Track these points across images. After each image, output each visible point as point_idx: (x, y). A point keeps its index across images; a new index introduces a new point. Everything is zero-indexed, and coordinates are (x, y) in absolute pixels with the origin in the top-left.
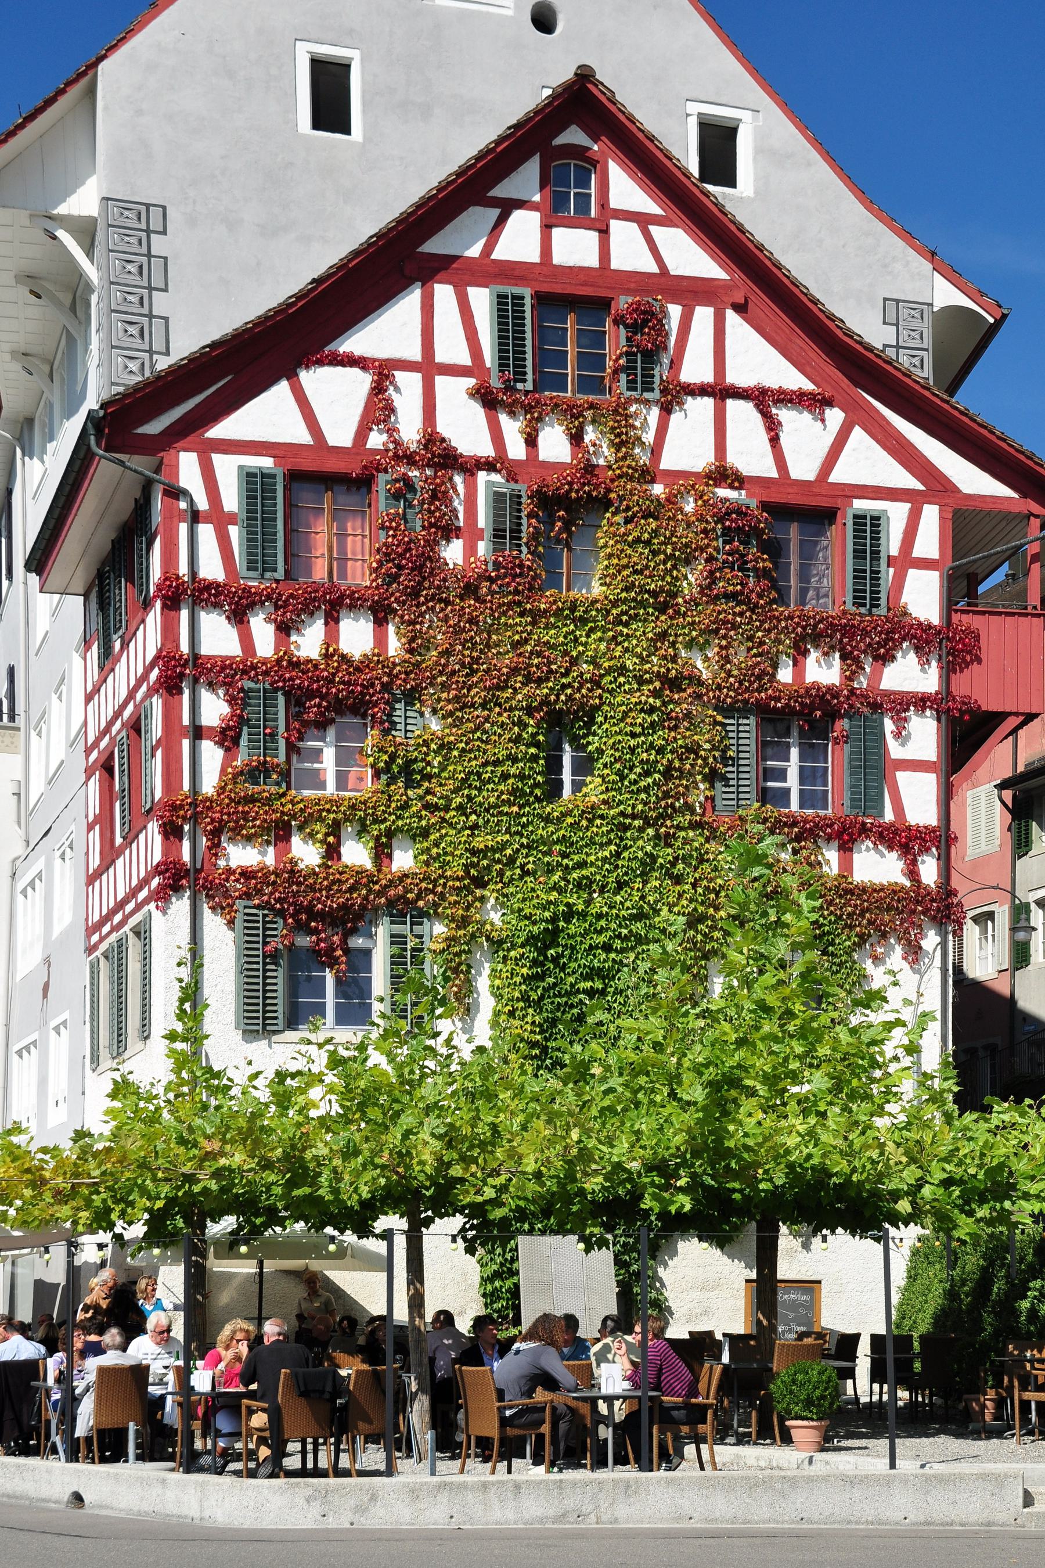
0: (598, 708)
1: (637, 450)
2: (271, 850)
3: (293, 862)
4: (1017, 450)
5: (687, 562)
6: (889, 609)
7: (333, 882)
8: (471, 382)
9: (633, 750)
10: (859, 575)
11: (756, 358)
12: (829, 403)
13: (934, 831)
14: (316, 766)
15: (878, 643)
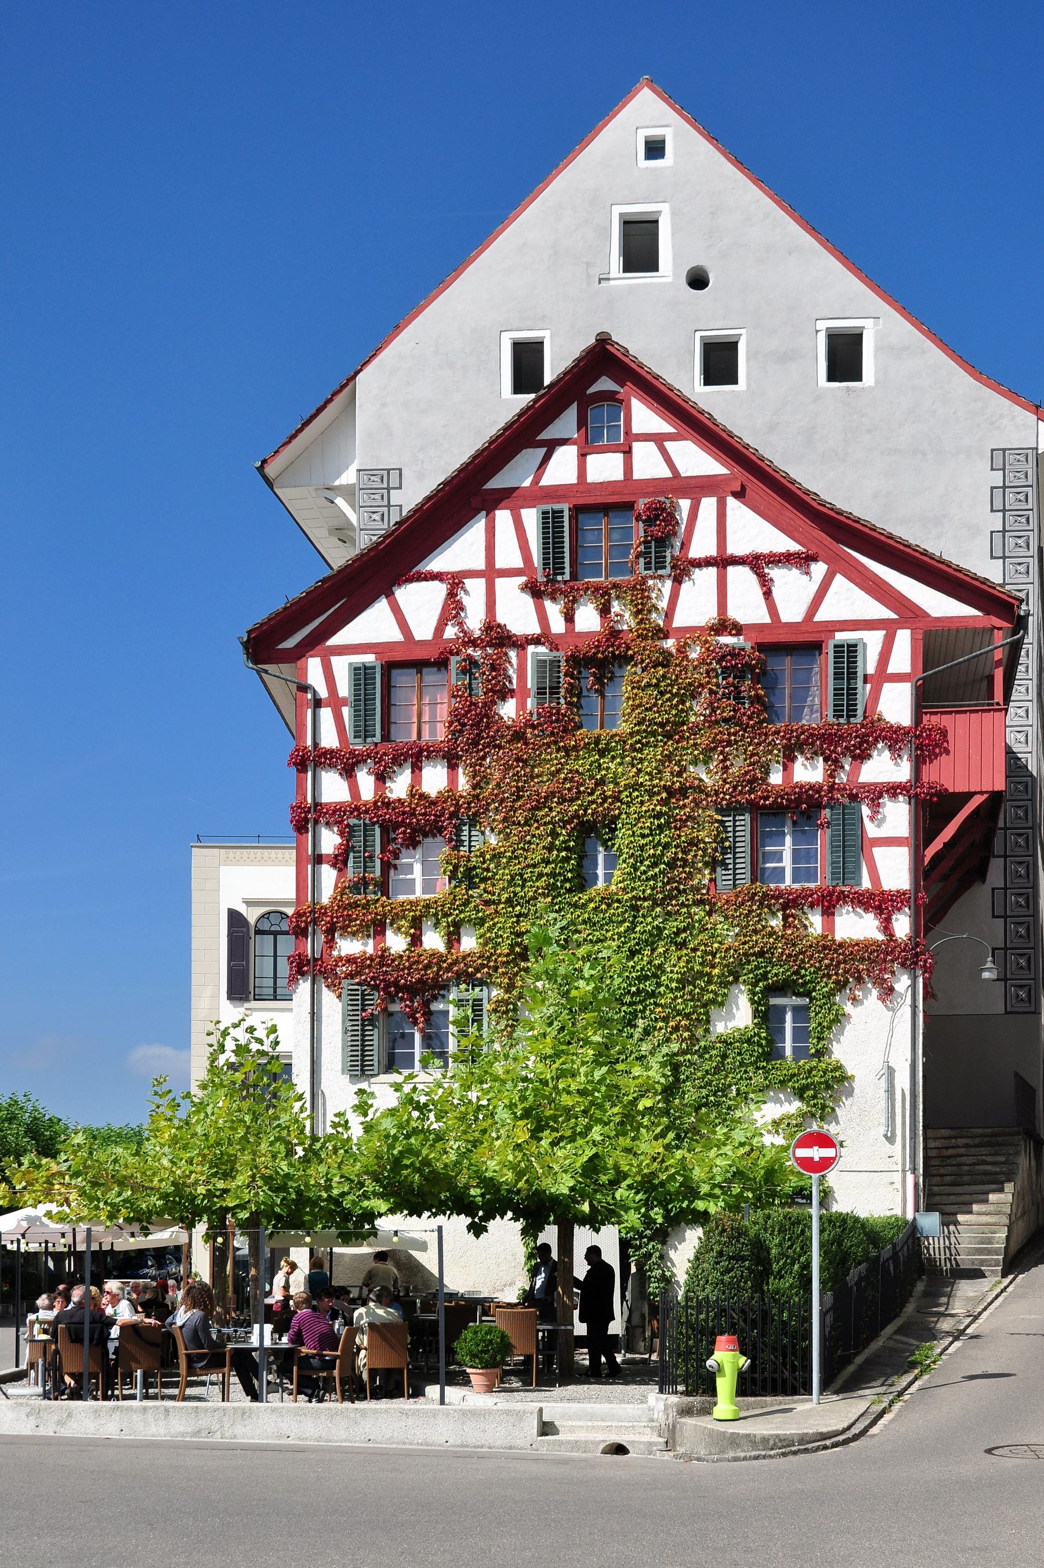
0: (618, 817)
1: (654, 615)
2: (371, 942)
3: (384, 950)
4: (972, 578)
5: (693, 697)
6: (865, 718)
7: (414, 963)
8: (523, 579)
9: (642, 848)
10: (838, 692)
11: (752, 531)
12: (814, 559)
13: (904, 894)
14: (409, 877)
15: (854, 745)
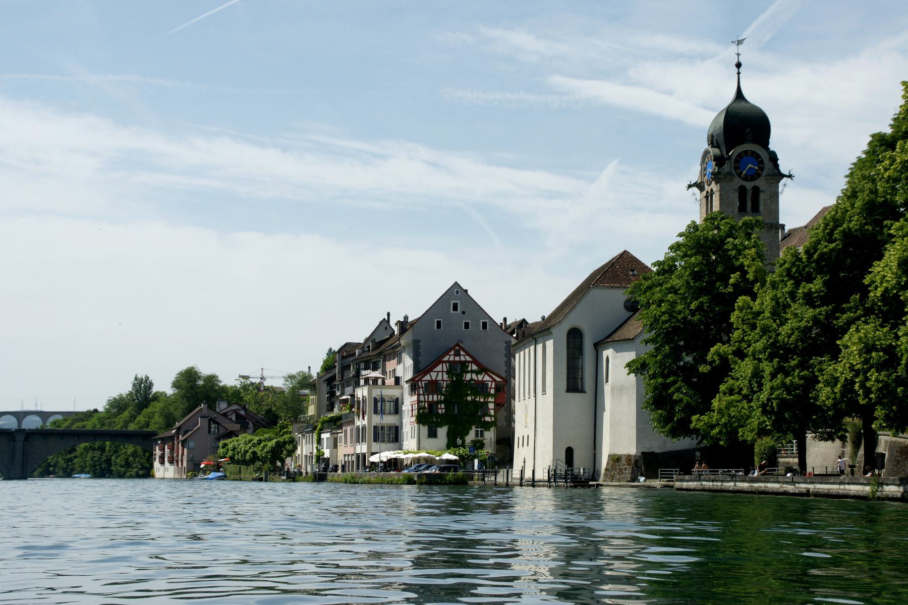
11: (475, 367)
